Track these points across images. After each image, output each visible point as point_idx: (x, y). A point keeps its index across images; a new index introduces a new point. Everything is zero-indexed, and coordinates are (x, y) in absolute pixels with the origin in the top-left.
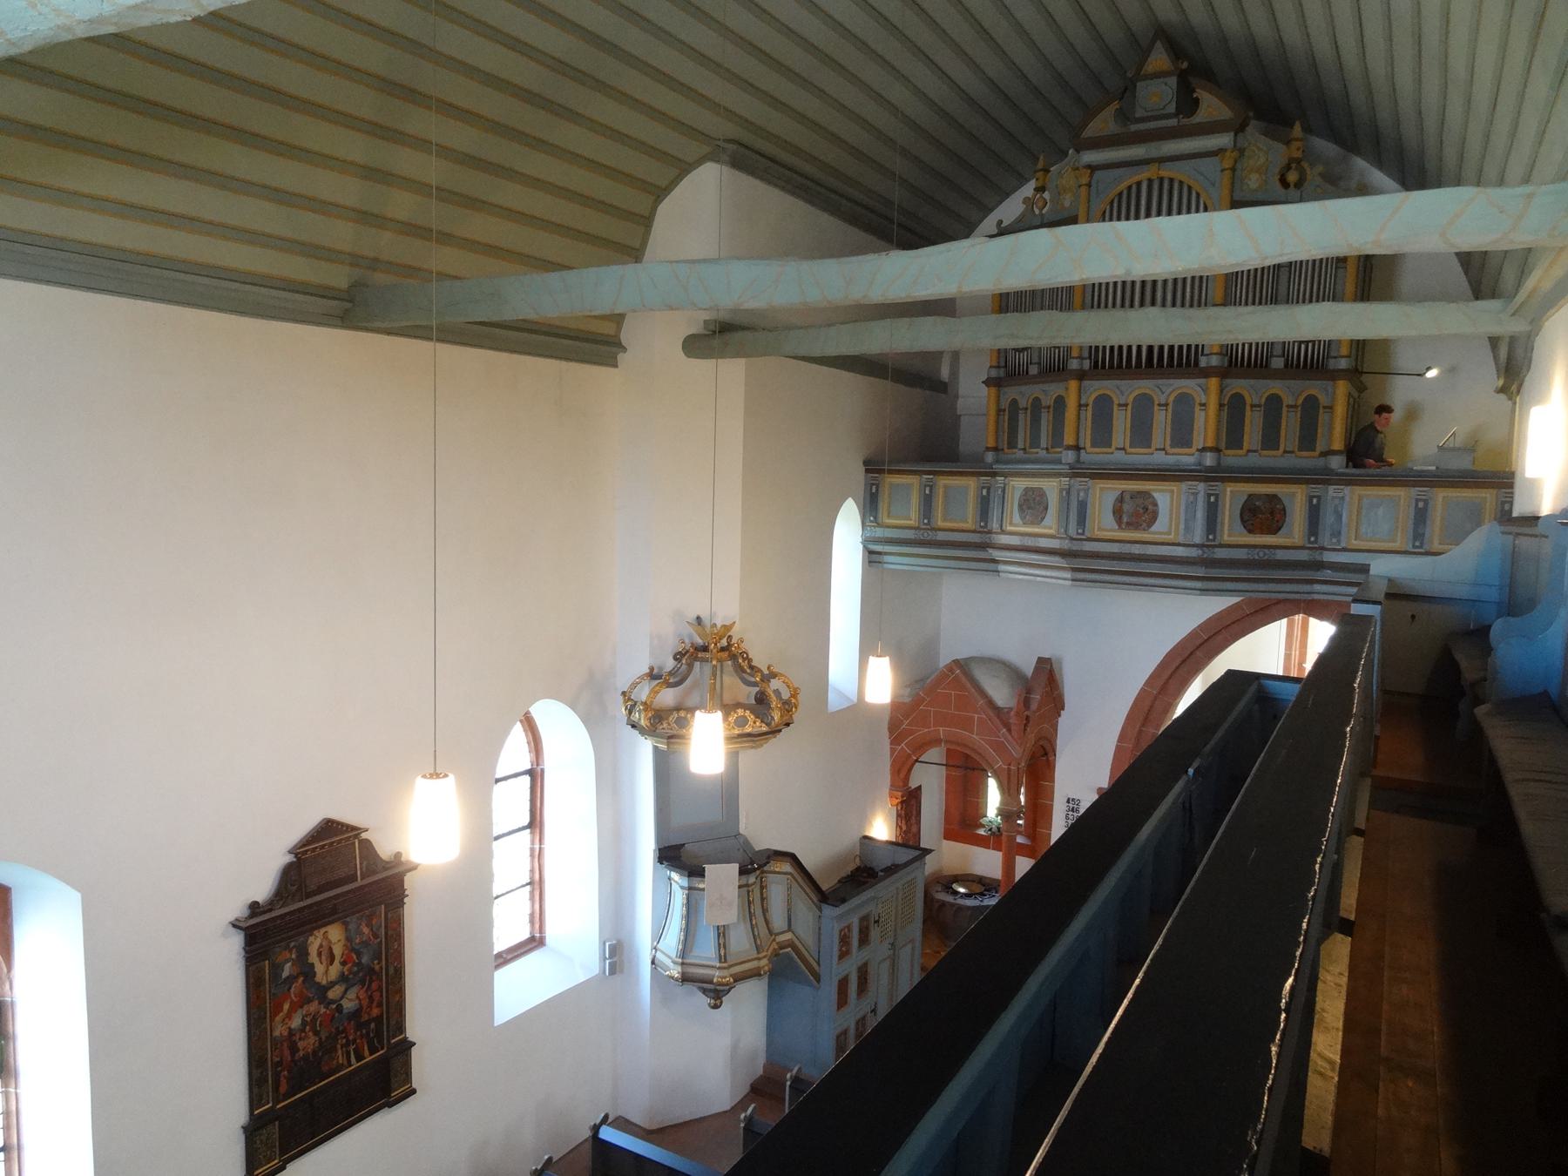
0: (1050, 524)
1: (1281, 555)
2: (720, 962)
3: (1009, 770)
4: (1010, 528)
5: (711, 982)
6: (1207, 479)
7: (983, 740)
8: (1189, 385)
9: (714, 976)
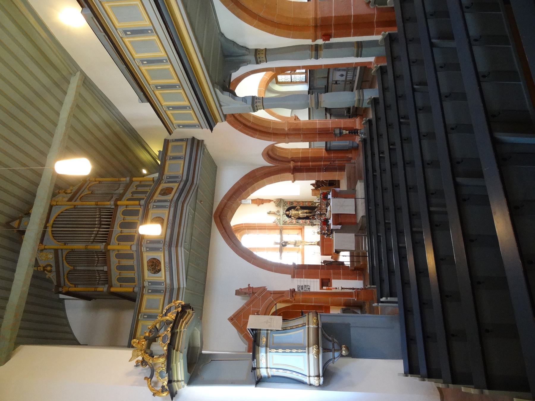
0: (160, 256)
1: (181, 187)
2: (305, 325)
4: (163, 278)
5: (317, 329)
7: (262, 306)
8: (120, 210)
9: (313, 328)
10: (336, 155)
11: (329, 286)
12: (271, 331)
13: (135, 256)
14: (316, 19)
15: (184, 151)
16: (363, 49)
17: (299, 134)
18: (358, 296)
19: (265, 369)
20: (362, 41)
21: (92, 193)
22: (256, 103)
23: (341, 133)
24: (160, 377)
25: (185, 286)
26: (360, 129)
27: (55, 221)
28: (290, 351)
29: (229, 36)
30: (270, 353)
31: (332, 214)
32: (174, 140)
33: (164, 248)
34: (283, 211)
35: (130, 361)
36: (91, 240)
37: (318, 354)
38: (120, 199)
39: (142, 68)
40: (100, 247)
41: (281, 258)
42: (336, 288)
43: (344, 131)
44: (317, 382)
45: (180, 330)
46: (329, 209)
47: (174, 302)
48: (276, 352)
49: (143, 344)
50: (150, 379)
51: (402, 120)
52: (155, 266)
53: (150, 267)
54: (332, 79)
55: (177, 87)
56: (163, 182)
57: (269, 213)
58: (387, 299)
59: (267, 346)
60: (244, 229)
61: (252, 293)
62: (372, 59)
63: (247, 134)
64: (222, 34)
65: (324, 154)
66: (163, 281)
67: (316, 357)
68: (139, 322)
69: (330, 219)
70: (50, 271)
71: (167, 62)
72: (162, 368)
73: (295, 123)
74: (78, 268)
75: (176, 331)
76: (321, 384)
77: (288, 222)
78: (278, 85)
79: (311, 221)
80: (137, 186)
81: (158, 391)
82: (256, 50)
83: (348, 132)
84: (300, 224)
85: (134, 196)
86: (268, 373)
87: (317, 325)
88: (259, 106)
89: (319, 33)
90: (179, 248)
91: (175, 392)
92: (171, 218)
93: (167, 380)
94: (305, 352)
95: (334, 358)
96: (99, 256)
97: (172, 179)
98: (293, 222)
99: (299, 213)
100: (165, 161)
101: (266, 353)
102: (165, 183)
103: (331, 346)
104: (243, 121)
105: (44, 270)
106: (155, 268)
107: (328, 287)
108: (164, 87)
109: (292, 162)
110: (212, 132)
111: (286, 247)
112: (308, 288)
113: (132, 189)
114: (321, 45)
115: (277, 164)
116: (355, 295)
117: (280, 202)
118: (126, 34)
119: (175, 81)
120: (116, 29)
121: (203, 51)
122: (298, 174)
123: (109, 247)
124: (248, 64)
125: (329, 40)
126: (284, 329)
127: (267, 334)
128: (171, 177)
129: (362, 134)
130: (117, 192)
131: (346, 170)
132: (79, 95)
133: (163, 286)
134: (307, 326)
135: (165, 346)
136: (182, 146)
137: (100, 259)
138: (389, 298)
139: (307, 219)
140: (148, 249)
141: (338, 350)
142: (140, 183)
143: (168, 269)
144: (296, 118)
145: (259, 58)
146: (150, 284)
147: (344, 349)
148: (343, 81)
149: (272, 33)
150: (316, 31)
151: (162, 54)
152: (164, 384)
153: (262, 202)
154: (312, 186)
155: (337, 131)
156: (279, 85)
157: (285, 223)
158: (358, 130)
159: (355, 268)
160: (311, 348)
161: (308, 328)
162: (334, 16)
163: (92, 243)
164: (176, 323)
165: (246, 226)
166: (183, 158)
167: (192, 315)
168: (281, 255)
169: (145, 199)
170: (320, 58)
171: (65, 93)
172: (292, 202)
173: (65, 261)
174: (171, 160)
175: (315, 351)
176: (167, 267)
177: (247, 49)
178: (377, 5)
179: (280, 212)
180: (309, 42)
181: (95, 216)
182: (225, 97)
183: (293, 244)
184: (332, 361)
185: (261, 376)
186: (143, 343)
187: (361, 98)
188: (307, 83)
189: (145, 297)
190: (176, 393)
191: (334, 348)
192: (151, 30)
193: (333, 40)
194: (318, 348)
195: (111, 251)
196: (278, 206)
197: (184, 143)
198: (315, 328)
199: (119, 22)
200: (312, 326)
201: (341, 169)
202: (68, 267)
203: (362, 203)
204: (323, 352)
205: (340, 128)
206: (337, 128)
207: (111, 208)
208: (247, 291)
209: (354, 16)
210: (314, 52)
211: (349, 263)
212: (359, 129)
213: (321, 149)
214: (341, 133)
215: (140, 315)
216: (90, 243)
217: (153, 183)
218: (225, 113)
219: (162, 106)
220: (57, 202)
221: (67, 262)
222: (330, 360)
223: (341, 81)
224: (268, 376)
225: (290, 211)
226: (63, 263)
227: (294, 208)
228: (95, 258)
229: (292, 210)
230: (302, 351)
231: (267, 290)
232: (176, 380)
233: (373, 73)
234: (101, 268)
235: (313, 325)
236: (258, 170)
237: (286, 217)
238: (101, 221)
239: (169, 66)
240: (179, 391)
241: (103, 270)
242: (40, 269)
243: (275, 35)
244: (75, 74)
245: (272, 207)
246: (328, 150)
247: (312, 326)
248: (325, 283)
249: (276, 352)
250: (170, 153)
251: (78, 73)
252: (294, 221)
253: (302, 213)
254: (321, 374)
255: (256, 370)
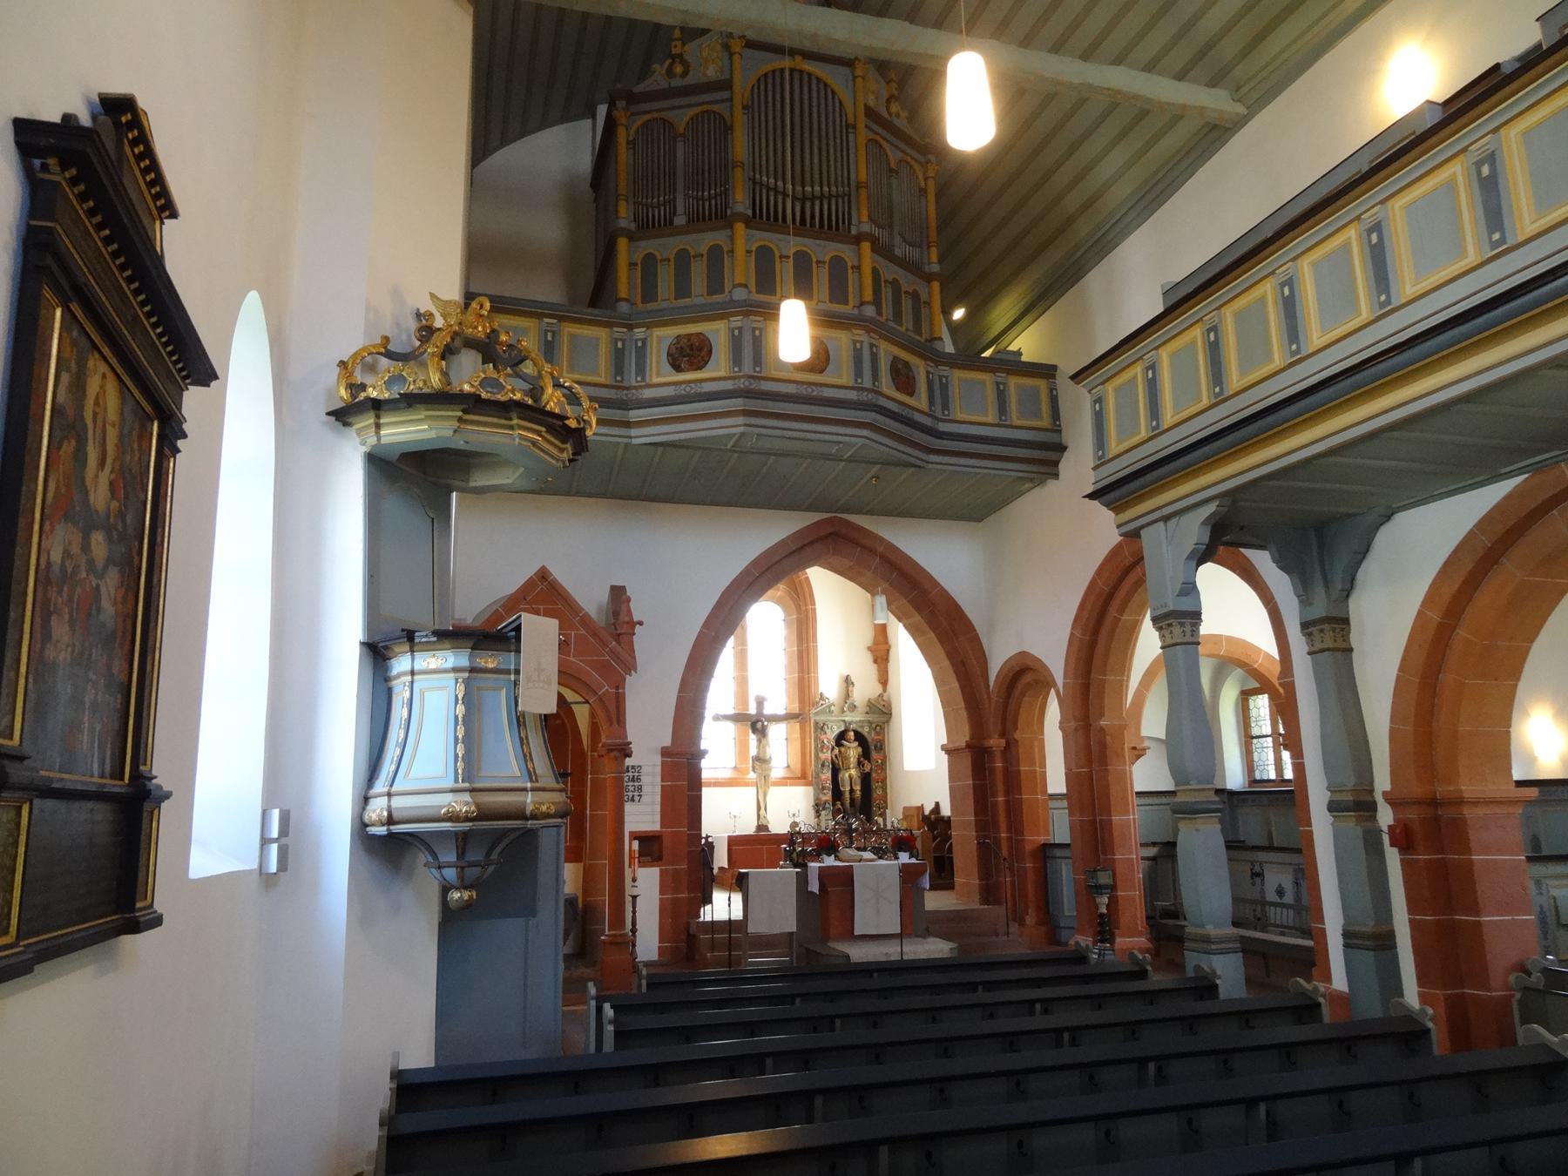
0: (718, 367)
1: (918, 417)
2: (531, 781)
3: (617, 693)
4: (656, 380)
5: (521, 815)
6: (868, 331)
7: (581, 661)
8: (846, 252)
9: (525, 802)
10: (1031, 876)
11: (642, 859)
12: (516, 683)
13: (718, 298)
14: (1459, 802)
15: (1023, 423)
16: (1371, 953)
17: (1090, 762)
18: (611, 943)
19: (409, 668)
20: (1396, 948)
21: (891, 170)
22: (1179, 623)
23: (1098, 889)
24: (389, 377)
25: (635, 441)
26: (1113, 950)
27: (810, 75)
28: (460, 737)
29: (1385, 538)
30: (454, 681)
31: (852, 866)
32: (1055, 392)
33: (739, 377)
34: (856, 722)
35: (432, 296)
36: (758, 176)
37: (452, 817)
38: (876, 249)
39: (1269, 285)
40: (740, 201)
41: (717, 718)
42: (634, 880)
43: (1106, 900)
44: (374, 817)
45: (516, 427)
46: (868, 855)
47: (591, 407)
48: (456, 696)
49: (476, 327)
50: (383, 350)
51: (1152, 1067)
52: (691, 354)
53: (686, 341)
54: (1266, 862)
55: (1215, 387)
56: (931, 367)
57: (848, 681)
58: (610, 1023)
59: (473, 670)
60: (798, 608)
61: (619, 632)
62: (1340, 982)
64: (1388, 517)
65: (1033, 839)
66: (648, 380)
67: (443, 812)
68: (534, 320)
69: (837, 858)
70: (670, 73)
71: (1293, 354)
72: (414, 381)
73: (1123, 749)
74: (680, 147)
75: (514, 415)
76: (368, 829)
77: (823, 736)
78: (1237, 699)
79: (827, 805)
80: (915, 296)
81: (351, 374)
82: (1345, 621)
83: (1104, 910)
84: (817, 774)
85: (885, 286)
86: (398, 676)
87: (531, 815)
88: (1171, 633)
89: (1412, 814)
90: (740, 420)
91: (350, 420)
92: (828, 393)
93: (381, 397)
94: (456, 781)
95: (440, 868)
96: (713, 202)
97: (940, 394)
98: (825, 751)
99: (849, 768)
100: (993, 371)
101: (455, 670)
102: (928, 373)
103: (475, 855)
104: (1122, 592)
105: (673, 57)
106: (684, 357)
107: (637, 855)
108: (1214, 349)
109: (1003, 742)
110: (1084, 497)
111: (750, 731)
112: (633, 796)
113: (908, 282)
114: (1373, 818)
115: (994, 697)
116: (615, 936)
117: (882, 712)
118: (1370, 231)
119: (1234, 380)
120: (1383, 202)
121: (1332, 459)
122: (966, 762)
123: (740, 227)
124: (1298, 596)
125: (1391, 846)
126: (521, 719)
127: (508, 672)
128: (944, 388)
129: (1099, 955)
130: (897, 240)
131: (986, 906)
132: (1177, 115)
133: (634, 381)
134: (529, 785)
135: (472, 386)
136: (1037, 414)
137: (707, 203)
138: (611, 1028)
139: (833, 792)
140: (736, 333)
141: (461, 877)
142: (925, 302)
143: (682, 390)
144: (1141, 753)
145: (1322, 631)
146: (640, 344)
147: (466, 895)
148: (1263, 897)
149: (1402, 668)
150: (1418, 802)
151: (1315, 337)
152: (371, 389)
153: (879, 660)
154: (933, 806)
155: (1104, 879)
156: (1237, 704)
157: (820, 728)
158: (1112, 942)
159: (694, 936)
160: (467, 797)
161: (525, 790)
162: (1471, 860)
163: (750, 179)
164: (533, 412)
165: (807, 616)
166: (1001, 419)
167: (558, 460)
168: (726, 717)
169: (878, 318)
170: (1332, 819)
171: (1180, 76)
172: (881, 749)
173: (699, 109)
174: (996, 387)
175: (461, 810)
176: (688, 389)
177: (1347, 592)
178: (1518, 996)
179: (853, 714)
180: (1382, 781)
181: (825, 183)
182: (1193, 530)
183: (758, 752)
184: (431, 859)
185: (390, 659)
186: (480, 329)
187: (1213, 947)
188: (1250, 787)
189: (602, 334)
190: (346, 424)
191: (469, 867)
192: (1388, 302)
193: (1393, 859)
194: (467, 819)
195: (728, 232)
196: (870, 708)
197: (1045, 422)
198: (525, 809)
199: (1407, 207)
200: (529, 800)
201: (989, 893)
202: (681, 119)
203: (886, 954)
204: (456, 833)
205: (1113, 887)
206: (1114, 879)
207: (850, 224)
208: (623, 617)
209: (1479, 921)
210: (1351, 799)
211: (708, 918)
212: (1117, 946)
213: (1047, 832)
214: (1098, 889)
215: (555, 321)
216: (752, 173)
217: (927, 340)
218: (1143, 532)
219: (1156, 348)
220: (863, 78)
221: (697, 115)
222: (434, 855)
224: (389, 677)
225: (857, 743)
226: (690, 106)
227: (866, 754)
228: (709, 191)
229: (860, 750)
230: (460, 771)
231: (628, 676)
232: (382, 421)
233: (1298, 982)
234: (680, 208)
235: (532, 802)
236: (976, 640)
237: (837, 731)
238: (813, 198)
239: (1278, 361)
240: (352, 432)
241: (675, 214)
242: (676, 46)
243: (1398, 678)
244: (1238, 101)
245: (866, 689)
246: (1046, 851)
247: (529, 800)
248: (650, 846)
249: (456, 696)
250: (1014, 382)
251: (1240, 109)
252: (827, 755)
253: (851, 778)
254: (396, 828)
255: (408, 643)
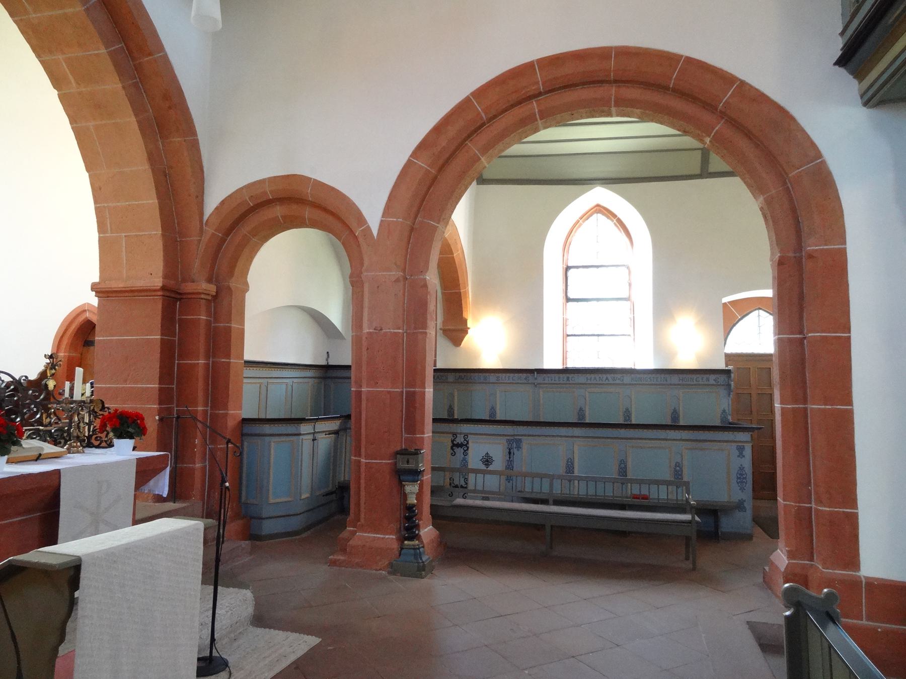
26: (423, 547)
63: (438, 129)
83: (412, 500)
109: (212, 289)
115: (209, 231)
212: (425, 542)
223: (464, 459)
236: (195, 146)
